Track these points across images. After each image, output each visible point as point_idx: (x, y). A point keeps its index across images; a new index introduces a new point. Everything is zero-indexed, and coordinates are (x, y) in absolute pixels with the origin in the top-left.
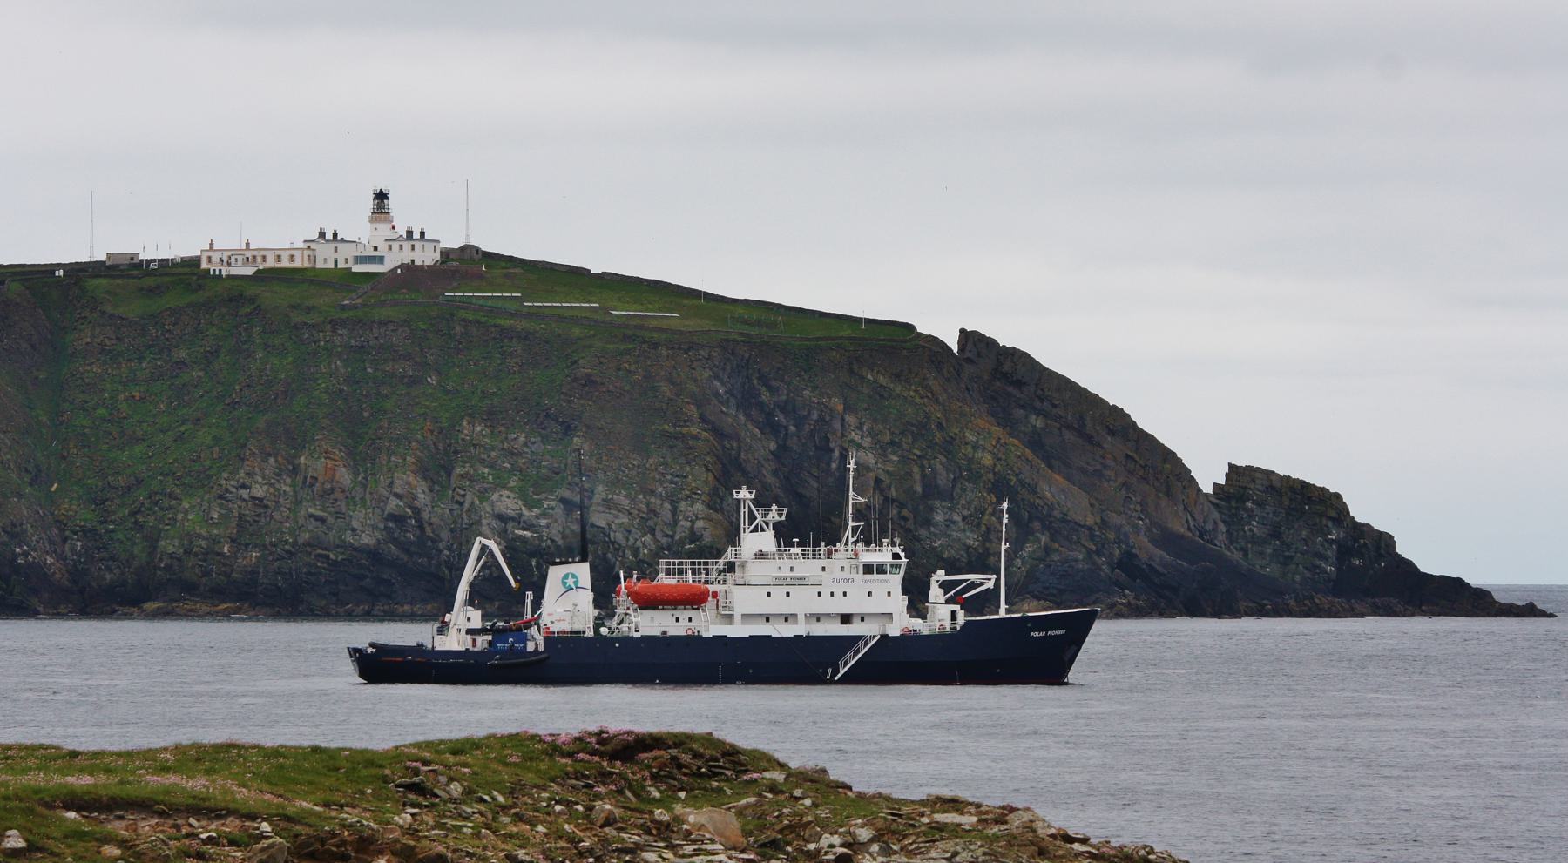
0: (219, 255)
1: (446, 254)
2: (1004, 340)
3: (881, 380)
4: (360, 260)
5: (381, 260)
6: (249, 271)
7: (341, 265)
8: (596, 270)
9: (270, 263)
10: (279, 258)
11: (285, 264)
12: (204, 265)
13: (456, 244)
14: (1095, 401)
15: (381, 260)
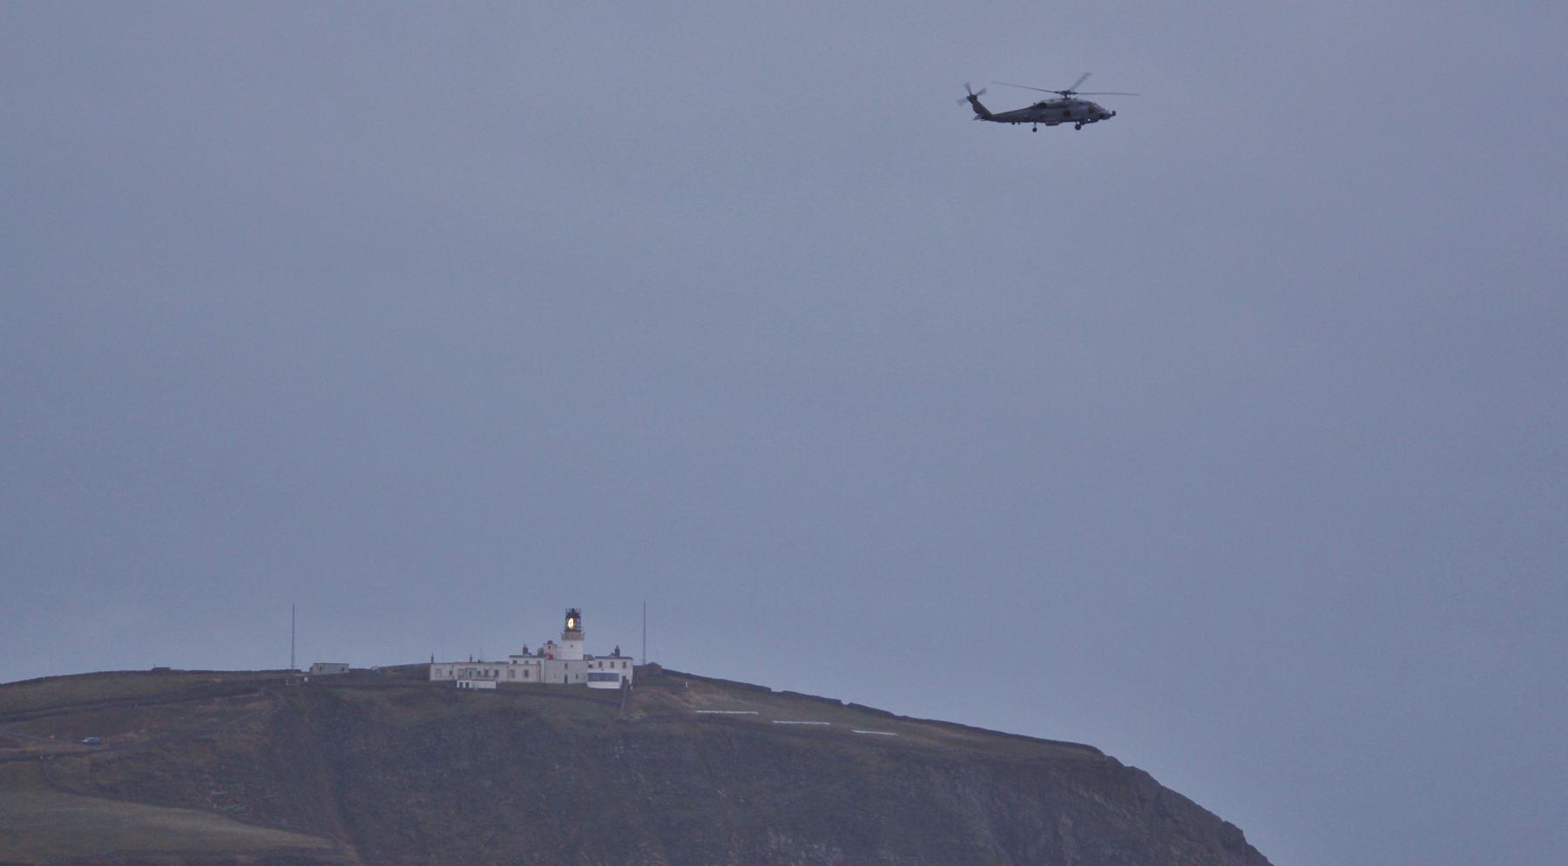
0: (449, 668)
1: (636, 669)
2: (1126, 762)
3: (1097, 798)
4: (592, 677)
5: (612, 678)
6: (492, 685)
7: (571, 681)
8: (776, 689)
9: (504, 677)
10: (512, 673)
11: (519, 678)
12: (433, 677)
13: (639, 663)
14: (1213, 819)
15: (612, 678)
